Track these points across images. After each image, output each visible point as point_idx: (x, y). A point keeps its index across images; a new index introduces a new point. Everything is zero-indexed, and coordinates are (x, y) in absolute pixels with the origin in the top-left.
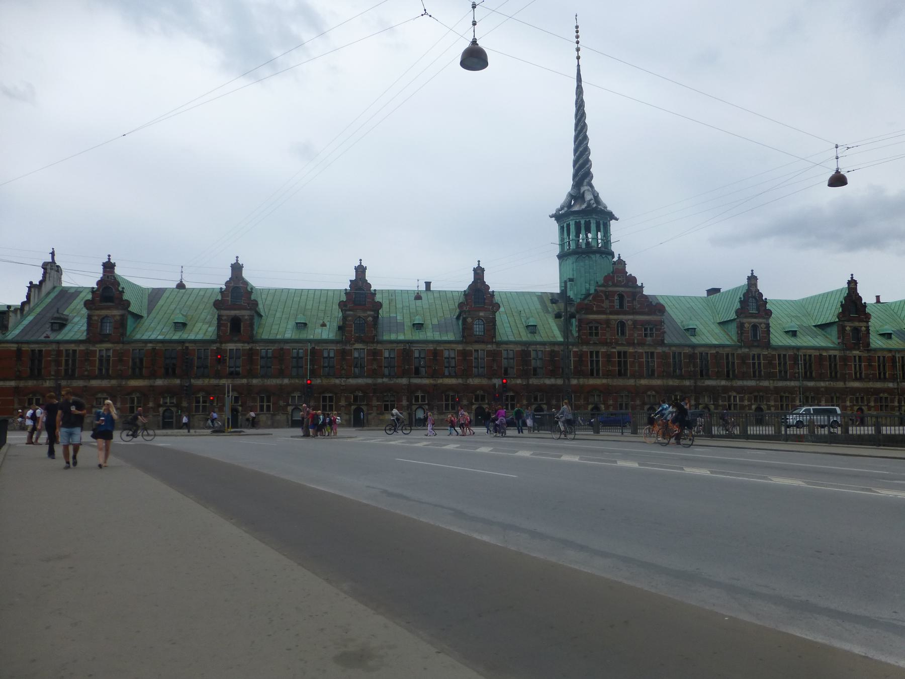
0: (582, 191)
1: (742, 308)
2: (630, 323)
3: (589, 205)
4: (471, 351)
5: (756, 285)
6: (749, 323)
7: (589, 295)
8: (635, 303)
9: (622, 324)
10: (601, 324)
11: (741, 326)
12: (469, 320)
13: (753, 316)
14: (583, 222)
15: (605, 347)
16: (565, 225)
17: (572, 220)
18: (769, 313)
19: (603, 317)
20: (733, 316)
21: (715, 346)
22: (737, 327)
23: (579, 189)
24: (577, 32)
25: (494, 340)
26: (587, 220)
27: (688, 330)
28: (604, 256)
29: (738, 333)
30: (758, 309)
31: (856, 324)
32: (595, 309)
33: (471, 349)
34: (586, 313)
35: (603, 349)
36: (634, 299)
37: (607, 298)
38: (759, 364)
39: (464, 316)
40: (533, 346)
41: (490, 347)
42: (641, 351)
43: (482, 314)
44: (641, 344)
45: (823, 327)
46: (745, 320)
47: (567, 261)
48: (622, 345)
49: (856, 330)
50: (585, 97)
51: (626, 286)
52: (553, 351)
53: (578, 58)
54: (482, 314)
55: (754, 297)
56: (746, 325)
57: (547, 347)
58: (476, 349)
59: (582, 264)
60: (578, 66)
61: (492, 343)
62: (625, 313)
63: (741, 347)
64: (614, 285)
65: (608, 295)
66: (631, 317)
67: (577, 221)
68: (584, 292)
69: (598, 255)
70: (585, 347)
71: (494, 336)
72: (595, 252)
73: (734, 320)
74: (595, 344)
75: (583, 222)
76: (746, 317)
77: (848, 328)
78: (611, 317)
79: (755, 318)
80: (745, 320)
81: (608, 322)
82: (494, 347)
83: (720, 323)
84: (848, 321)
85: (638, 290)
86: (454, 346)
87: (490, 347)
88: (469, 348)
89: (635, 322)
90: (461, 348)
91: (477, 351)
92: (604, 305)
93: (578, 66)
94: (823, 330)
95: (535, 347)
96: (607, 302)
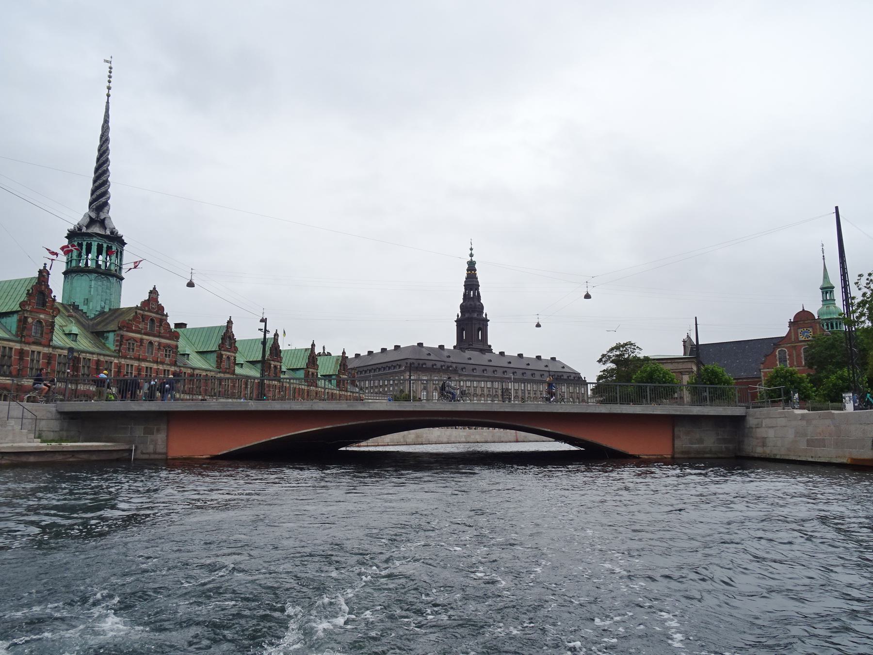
0: (102, 217)
1: (222, 343)
2: (156, 344)
3: (112, 233)
4: (28, 351)
5: (231, 327)
6: (226, 355)
7: (104, 312)
8: (162, 328)
9: (151, 343)
10: (137, 342)
11: (220, 357)
12: (30, 320)
13: (227, 350)
14: (105, 245)
15: (137, 362)
16: (85, 243)
17: (95, 241)
18: (236, 350)
19: (138, 336)
20: (215, 348)
21: (206, 370)
22: (217, 357)
23: (98, 214)
24: (110, 72)
25: (51, 344)
26: (89, 242)
27: (184, 355)
28: (118, 280)
29: (217, 361)
30: (230, 345)
31: (276, 363)
32: (134, 328)
33: (28, 349)
34: (127, 331)
35: (136, 363)
36: (161, 325)
37: (143, 321)
38: (228, 385)
39: (26, 315)
40: (83, 354)
41: (46, 350)
42: (161, 368)
43: (42, 316)
44: (162, 363)
45: (253, 363)
46: (223, 353)
47: (83, 278)
48: (149, 361)
49: (275, 367)
50: (111, 135)
51: (157, 313)
52: (98, 361)
53: (108, 96)
54: (42, 316)
55: (229, 337)
56: (224, 356)
57: (94, 356)
58: (33, 350)
59: (100, 283)
60: (108, 102)
61: (49, 346)
62: (155, 336)
63: (220, 372)
64: (149, 311)
65: (144, 318)
66: (157, 339)
67: (110, 245)
68: (99, 309)
69: (115, 279)
70: (123, 360)
71: (51, 340)
72: (113, 276)
73: (215, 351)
74: (131, 358)
75: (105, 245)
76: (224, 351)
77: (272, 366)
78: (145, 337)
79: (229, 352)
80: (223, 353)
81: (142, 340)
82: (51, 350)
83: (198, 352)
84: (273, 361)
85: (164, 317)
86: (12, 344)
87: (46, 350)
88: (27, 348)
89: (160, 344)
90: (19, 348)
91: (33, 352)
92: (140, 326)
93: (108, 102)
94: (253, 365)
95: (85, 354)
96: (143, 323)
